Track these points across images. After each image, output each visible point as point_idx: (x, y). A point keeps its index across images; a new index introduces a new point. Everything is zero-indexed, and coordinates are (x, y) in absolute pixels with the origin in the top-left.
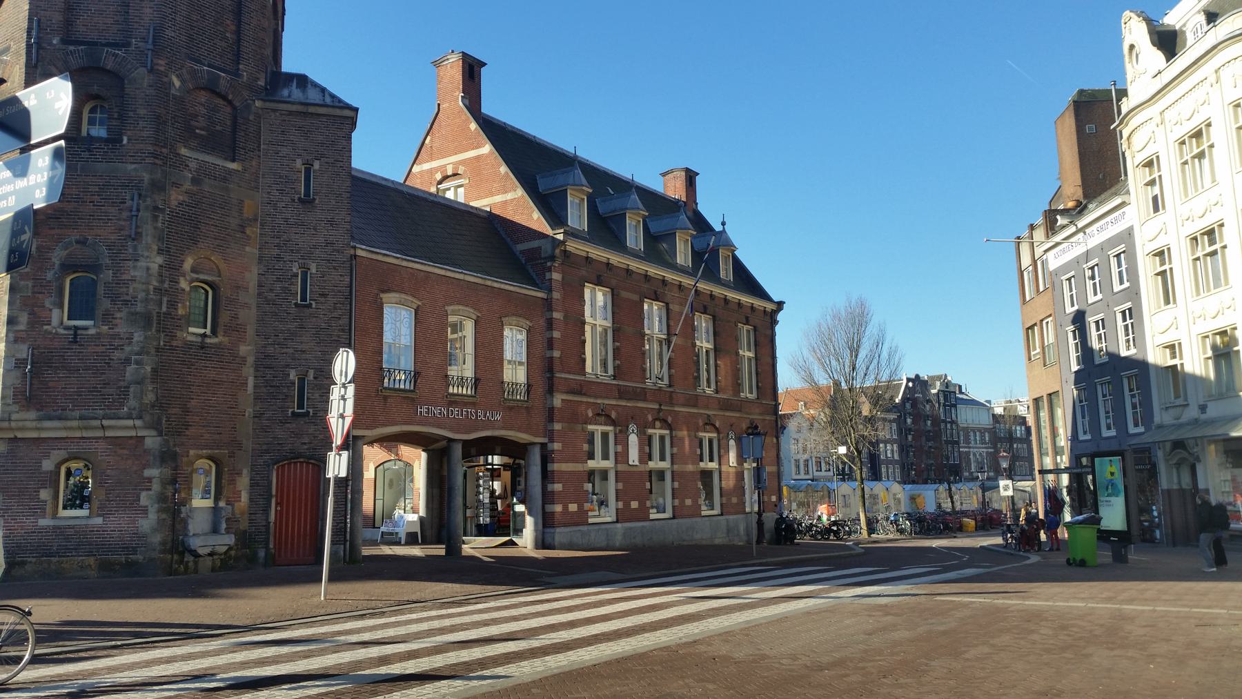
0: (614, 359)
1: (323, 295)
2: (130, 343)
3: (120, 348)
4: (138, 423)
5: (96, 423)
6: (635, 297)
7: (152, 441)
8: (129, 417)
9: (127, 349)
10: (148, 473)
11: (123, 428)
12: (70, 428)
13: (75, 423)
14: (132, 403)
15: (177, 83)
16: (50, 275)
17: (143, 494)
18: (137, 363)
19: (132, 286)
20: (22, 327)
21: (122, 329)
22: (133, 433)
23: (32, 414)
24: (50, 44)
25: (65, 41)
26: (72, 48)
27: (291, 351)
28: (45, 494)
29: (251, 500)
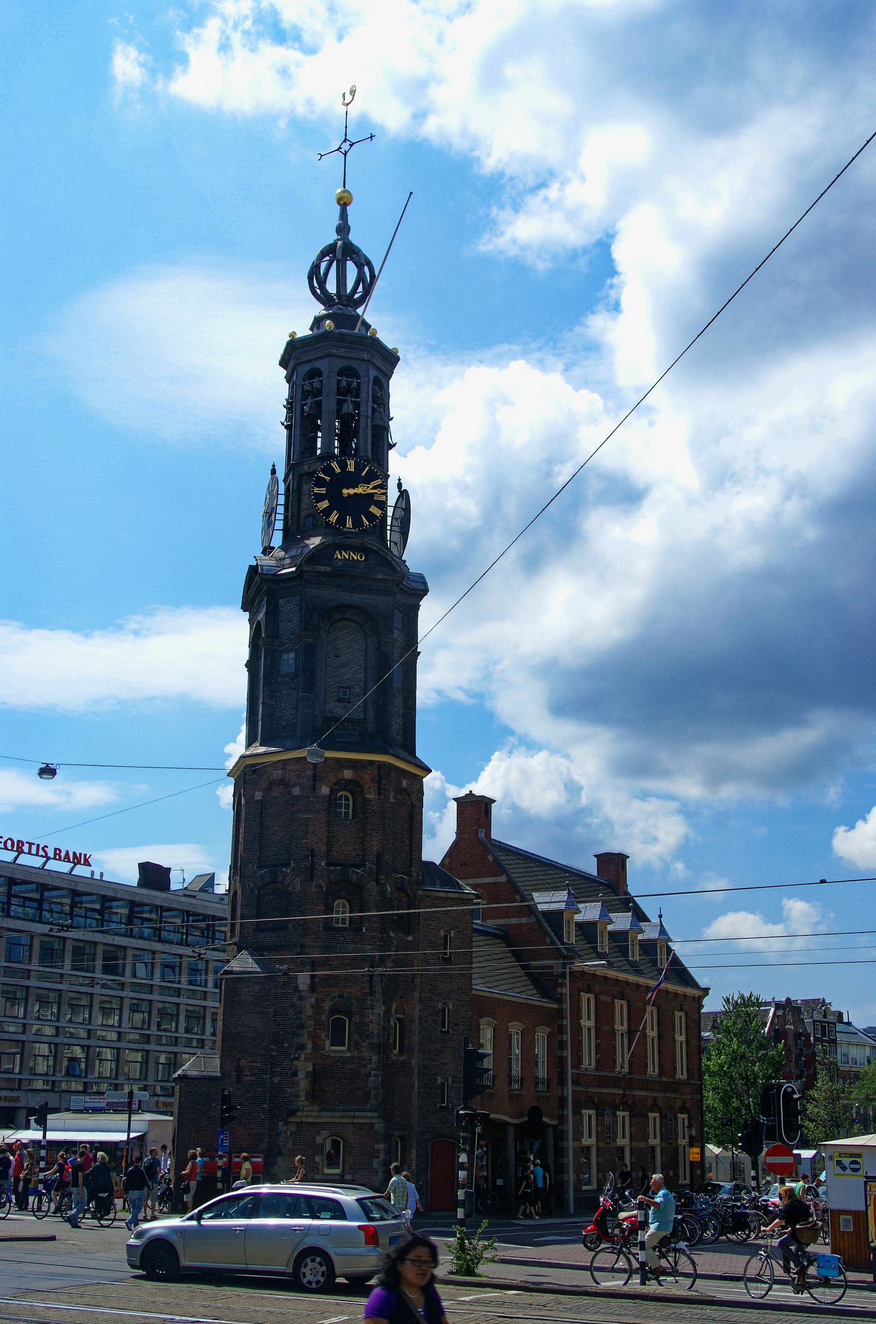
0: (596, 1054)
1: (457, 1025)
2: (370, 1063)
3: (365, 1066)
4: (376, 1114)
5: (352, 1114)
6: (609, 999)
7: (379, 1126)
8: (371, 1111)
9: (369, 1066)
10: (377, 1147)
11: (363, 1117)
12: (336, 1117)
13: (338, 1114)
14: (373, 1101)
15: (389, 889)
16: (323, 1018)
17: (375, 1160)
18: (375, 1076)
19: (371, 1025)
20: (309, 1051)
21: (366, 1054)
22: (369, 1121)
23: (316, 1108)
24: (320, 865)
25: (329, 864)
26: (332, 868)
27: (438, 1063)
28: (318, 1159)
29: (417, 1165)
